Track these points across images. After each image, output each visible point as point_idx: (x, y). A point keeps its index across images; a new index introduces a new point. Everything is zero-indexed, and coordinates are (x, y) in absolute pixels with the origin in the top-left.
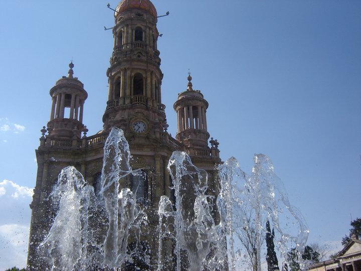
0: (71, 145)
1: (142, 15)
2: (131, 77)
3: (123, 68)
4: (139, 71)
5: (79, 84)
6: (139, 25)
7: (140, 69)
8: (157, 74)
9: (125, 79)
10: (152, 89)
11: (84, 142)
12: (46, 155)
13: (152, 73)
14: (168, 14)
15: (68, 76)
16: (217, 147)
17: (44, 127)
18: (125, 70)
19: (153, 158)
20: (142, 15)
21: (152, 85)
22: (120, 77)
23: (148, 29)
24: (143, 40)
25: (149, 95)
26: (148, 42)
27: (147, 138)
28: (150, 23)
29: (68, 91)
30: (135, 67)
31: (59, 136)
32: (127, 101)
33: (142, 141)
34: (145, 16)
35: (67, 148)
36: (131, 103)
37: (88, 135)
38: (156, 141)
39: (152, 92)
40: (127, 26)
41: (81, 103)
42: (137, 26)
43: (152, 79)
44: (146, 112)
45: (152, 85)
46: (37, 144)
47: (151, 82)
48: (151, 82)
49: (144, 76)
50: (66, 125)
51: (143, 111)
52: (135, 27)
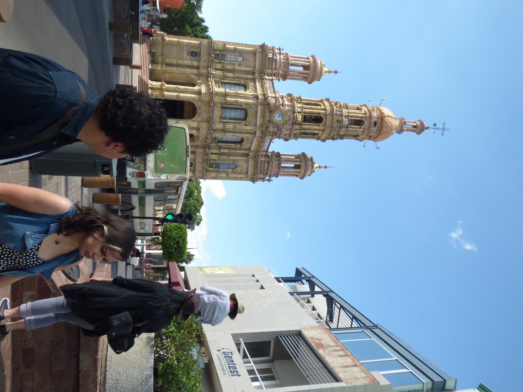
0: (268, 69)
1: (375, 126)
2: (319, 113)
3: (327, 108)
4: (324, 120)
5: (318, 77)
6: (366, 123)
7: (326, 122)
8: (323, 135)
9: (318, 109)
10: (310, 129)
11: (270, 78)
12: (260, 50)
13: (324, 131)
14: (378, 148)
15: (325, 69)
16: (267, 180)
17: (282, 50)
18: (325, 110)
19: (256, 125)
20: (375, 126)
21: (314, 130)
22: (321, 106)
23: (362, 130)
24: (353, 126)
25: (304, 126)
26: (350, 129)
27: (270, 121)
28: (368, 132)
29: (312, 68)
30: (328, 118)
31: (276, 60)
32: (300, 110)
33: (267, 118)
34: (375, 129)
35: (267, 66)
36: (298, 112)
37: (276, 82)
38: (267, 127)
39: (308, 129)
40: (365, 114)
41: (305, 79)
42: (365, 121)
43: (319, 130)
44: (290, 122)
45: (314, 130)
46: (269, 44)
47: (316, 130)
48: (316, 130)
49: (321, 124)
50: (285, 66)
51: (291, 120)
52: (364, 119)
